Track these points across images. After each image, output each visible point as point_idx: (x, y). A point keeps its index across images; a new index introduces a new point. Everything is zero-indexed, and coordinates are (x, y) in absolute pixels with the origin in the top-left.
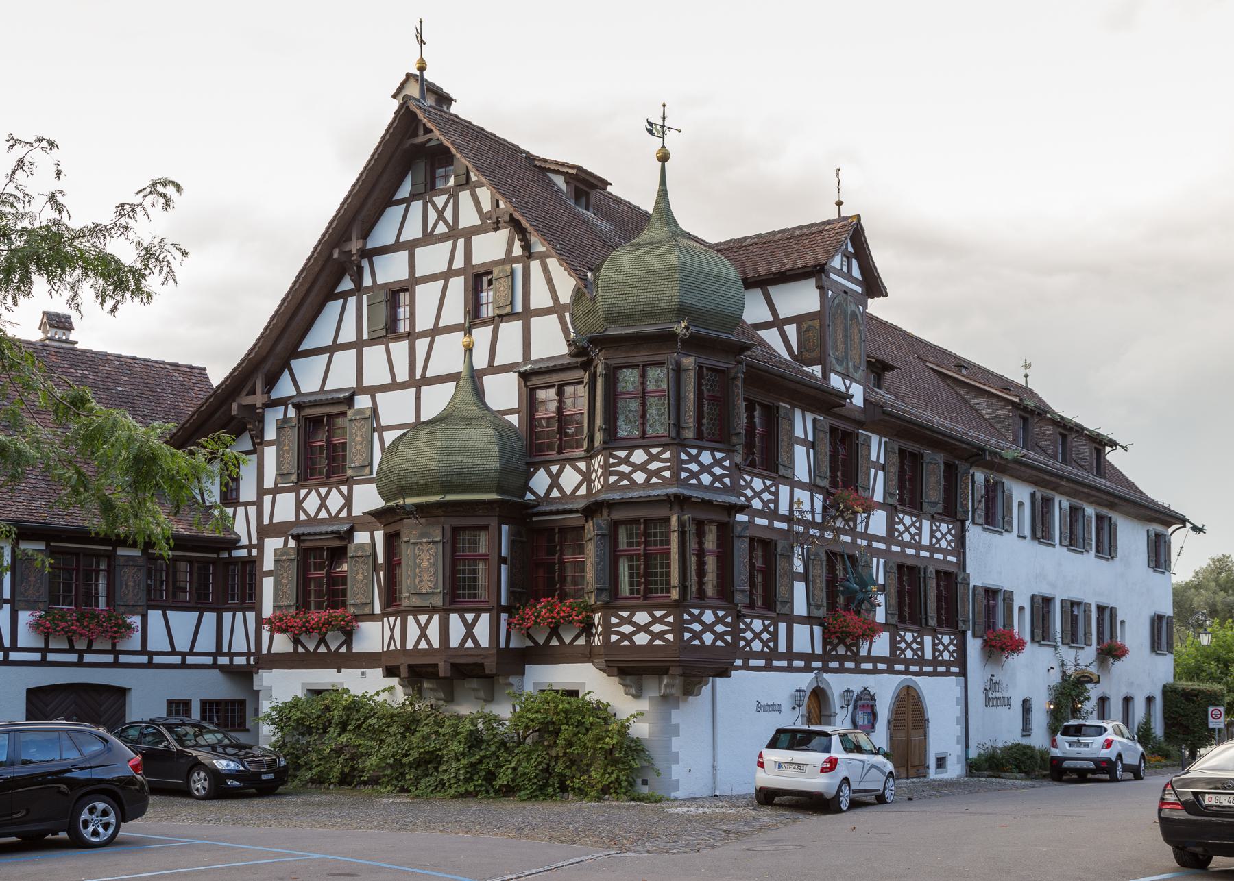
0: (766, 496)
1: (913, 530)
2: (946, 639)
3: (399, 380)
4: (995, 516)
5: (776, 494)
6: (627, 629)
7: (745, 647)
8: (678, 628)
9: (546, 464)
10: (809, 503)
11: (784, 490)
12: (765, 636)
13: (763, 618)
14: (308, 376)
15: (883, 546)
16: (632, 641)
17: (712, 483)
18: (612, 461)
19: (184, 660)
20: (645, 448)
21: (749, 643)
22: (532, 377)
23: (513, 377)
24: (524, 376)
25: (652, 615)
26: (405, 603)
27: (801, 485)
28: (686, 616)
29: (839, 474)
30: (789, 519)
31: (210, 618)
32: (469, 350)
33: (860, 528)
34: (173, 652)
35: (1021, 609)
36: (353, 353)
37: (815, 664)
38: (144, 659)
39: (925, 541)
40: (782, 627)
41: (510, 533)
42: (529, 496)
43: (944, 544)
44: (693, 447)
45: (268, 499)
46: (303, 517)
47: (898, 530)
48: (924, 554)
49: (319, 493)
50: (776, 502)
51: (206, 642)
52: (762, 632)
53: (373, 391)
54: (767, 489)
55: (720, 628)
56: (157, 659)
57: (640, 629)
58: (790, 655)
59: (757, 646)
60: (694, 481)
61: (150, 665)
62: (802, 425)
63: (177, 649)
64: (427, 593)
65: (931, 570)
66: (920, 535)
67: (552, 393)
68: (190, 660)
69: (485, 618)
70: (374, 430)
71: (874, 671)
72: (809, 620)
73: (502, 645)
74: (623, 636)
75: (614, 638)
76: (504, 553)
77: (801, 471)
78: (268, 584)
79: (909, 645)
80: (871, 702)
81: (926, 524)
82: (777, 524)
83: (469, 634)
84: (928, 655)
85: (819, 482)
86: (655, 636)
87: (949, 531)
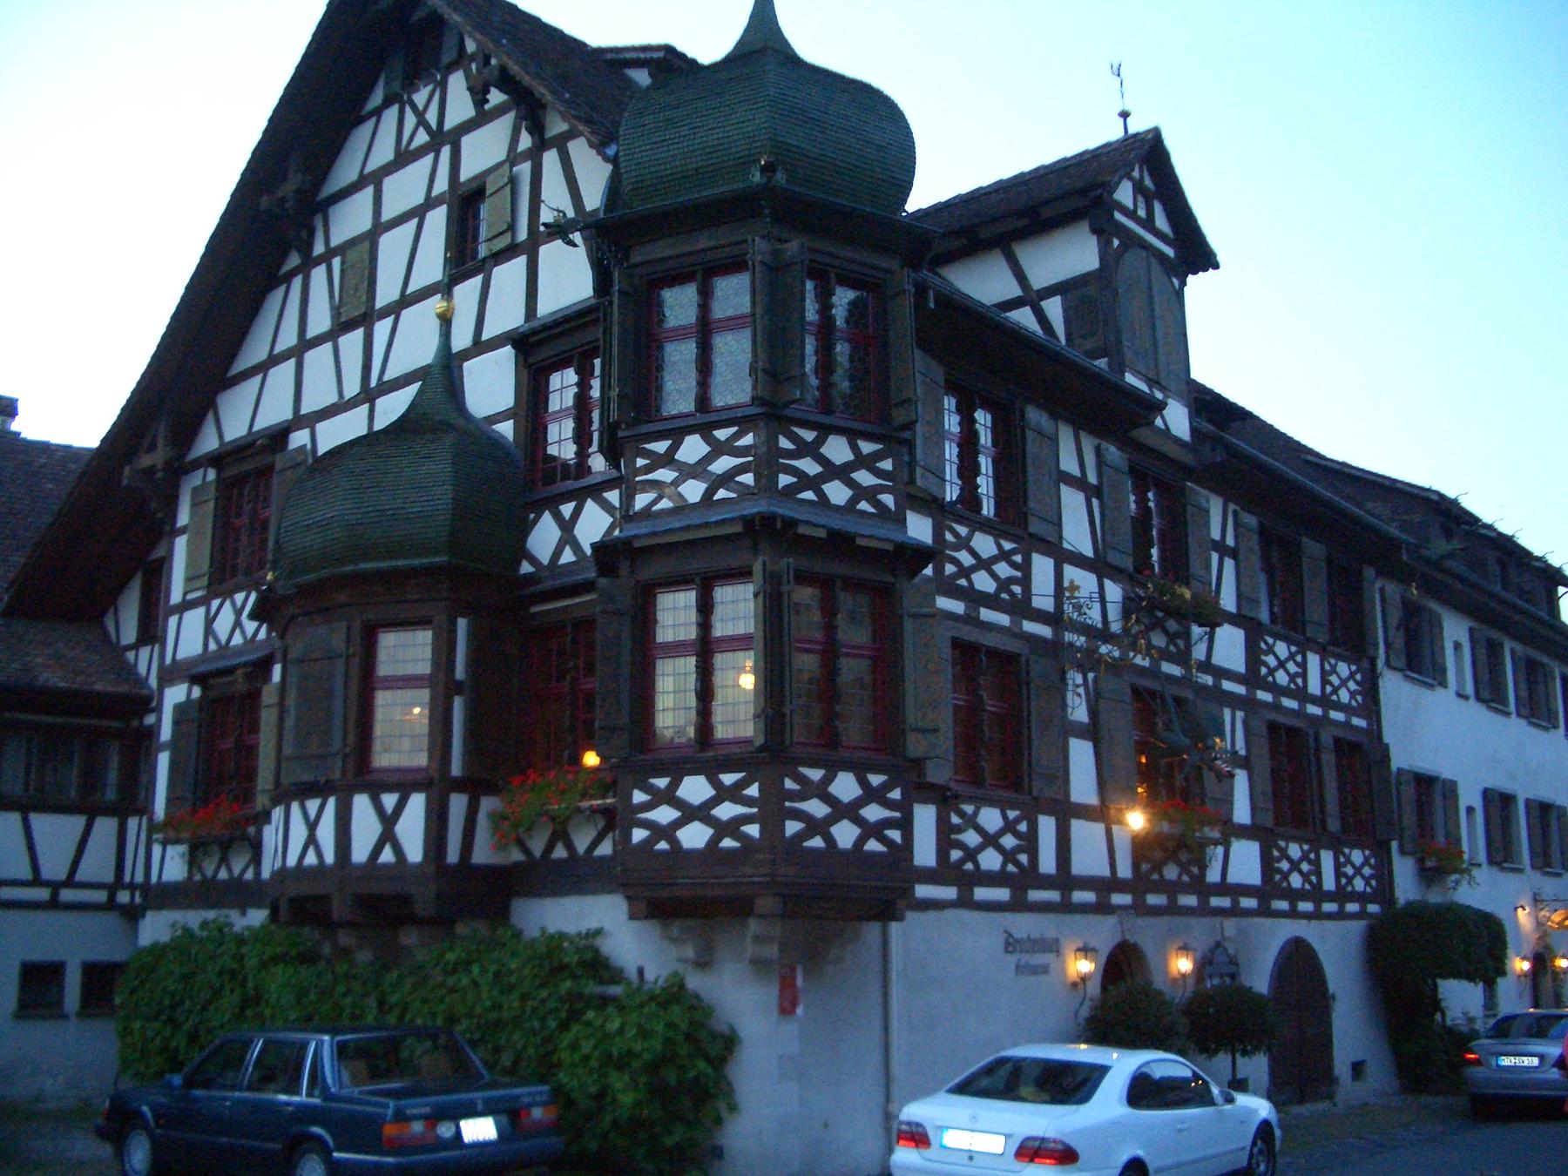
0: (1003, 570)
1: (1292, 667)
2: (1357, 856)
4: (1421, 663)
5: (1026, 568)
6: (664, 815)
7: (962, 861)
8: (773, 810)
9: (552, 503)
10: (1099, 599)
11: (1042, 566)
12: (1009, 841)
13: (1003, 806)
14: (239, 415)
15: (1240, 690)
16: (674, 842)
17: (853, 501)
18: (640, 462)
19: (55, 895)
20: (705, 430)
21: (971, 854)
22: (539, 348)
23: (508, 351)
25: (716, 784)
27: (1079, 560)
28: (789, 784)
29: (1154, 552)
30: (1054, 618)
31: (105, 827)
33: (1199, 652)
34: (37, 881)
35: (1470, 810)
37: (1120, 899)
39: (1314, 687)
40: (1047, 826)
41: (472, 634)
42: (526, 568)
43: (1344, 696)
45: (173, 621)
46: (212, 646)
47: (1266, 664)
48: (1313, 710)
49: (233, 604)
50: (1026, 581)
51: (97, 865)
52: (1001, 833)
54: (1004, 556)
55: (873, 813)
57: (691, 813)
58: (1065, 879)
59: (990, 860)
60: (809, 495)
62: (1071, 452)
65: (1326, 738)
66: (1304, 675)
67: (570, 376)
68: (67, 895)
71: (1235, 911)
73: (453, 855)
75: (639, 835)
76: (460, 672)
77: (1077, 533)
78: (164, 759)
79: (1295, 866)
80: (1232, 969)
81: (1313, 660)
82: (1029, 626)
83: (388, 836)
84: (1329, 883)
85: (1115, 558)
86: (724, 828)
87: (1352, 676)
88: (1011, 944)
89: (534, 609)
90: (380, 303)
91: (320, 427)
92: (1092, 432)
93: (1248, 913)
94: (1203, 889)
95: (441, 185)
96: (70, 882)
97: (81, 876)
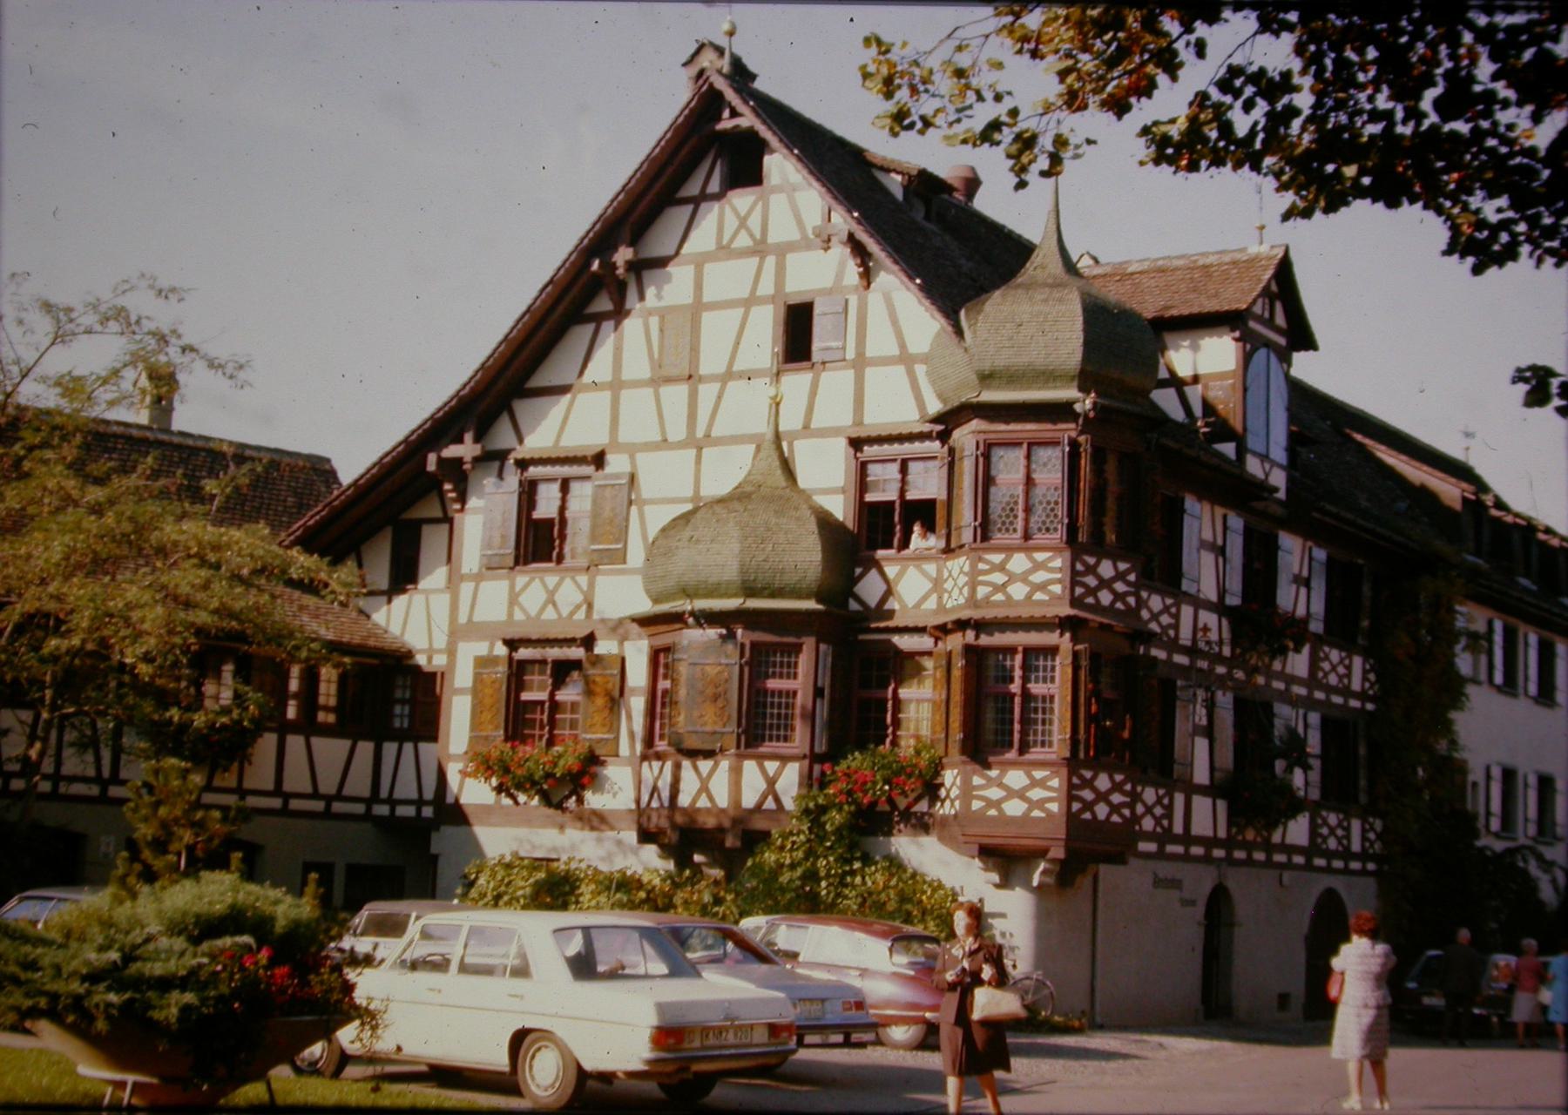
1: (1341, 670)
3: (670, 439)
5: (1177, 616)
11: (1187, 611)
16: (1000, 810)
19: (328, 806)
24: (856, 444)
30: (1192, 651)
34: (315, 795)
36: (606, 396)
38: (276, 803)
40: (1179, 799)
44: (1091, 555)
50: (1176, 627)
51: (359, 784)
53: (632, 450)
56: (295, 804)
57: (1011, 793)
58: (1187, 838)
61: (285, 812)
63: (323, 789)
66: (1349, 676)
67: (893, 470)
68: (338, 807)
72: (1211, 791)
74: (990, 803)
75: (976, 805)
88: (1158, 882)
89: (861, 637)
90: (704, 369)
91: (639, 457)
92: (1222, 505)
93: (1297, 867)
94: (1269, 848)
95: (767, 287)
96: (339, 796)
97: (347, 791)
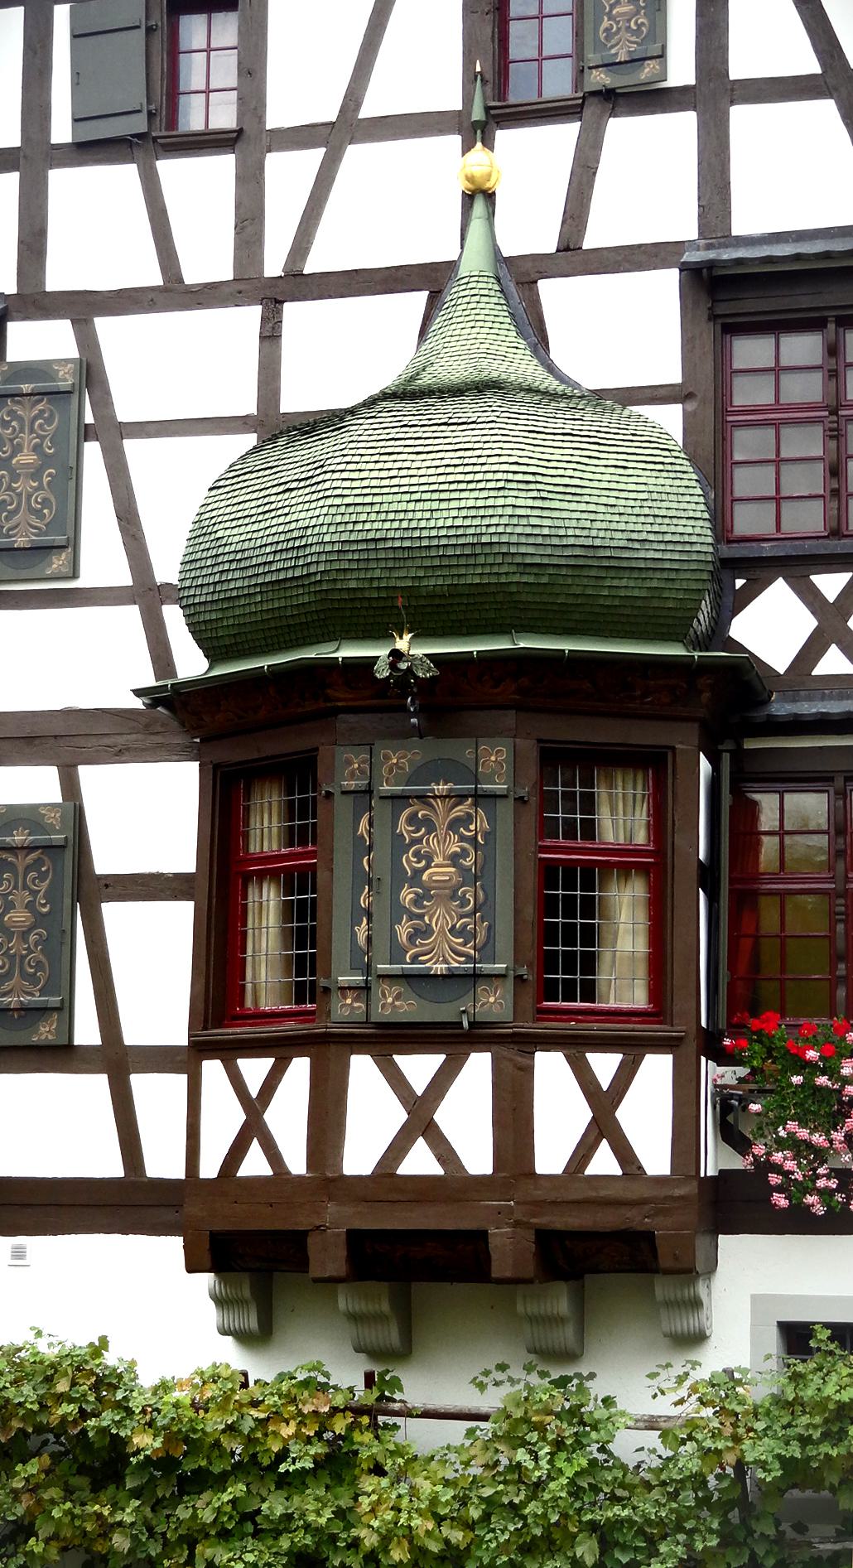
3: (193, 274)
23: (668, 280)
26: (346, 1009)
32: (479, 197)
53: (83, 308)
64: (451, 976)
69: (657, 1069)
70: (87, 433)
90: (277, 116)
